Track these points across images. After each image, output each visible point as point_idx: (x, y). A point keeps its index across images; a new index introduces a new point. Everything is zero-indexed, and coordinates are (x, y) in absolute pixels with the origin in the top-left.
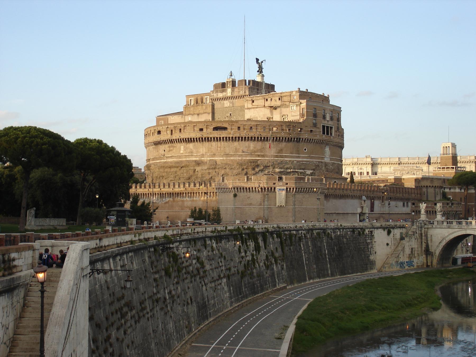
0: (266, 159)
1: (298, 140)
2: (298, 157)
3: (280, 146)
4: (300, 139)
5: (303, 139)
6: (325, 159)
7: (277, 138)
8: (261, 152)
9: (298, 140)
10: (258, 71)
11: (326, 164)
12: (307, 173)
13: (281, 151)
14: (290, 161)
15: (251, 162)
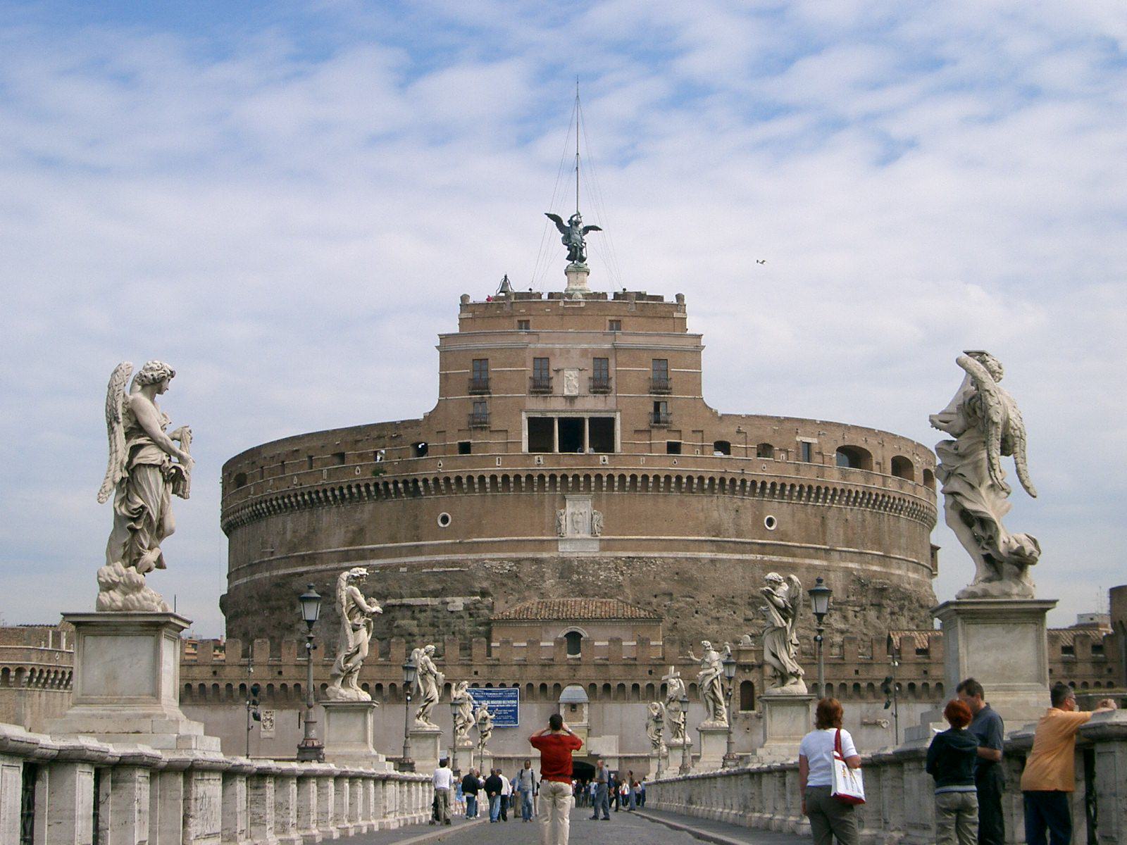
0: (320, 567)
1: (412, 488)
2: (417, 550)
3: (358, 515)
4: (415, 481)
5: (425, 481)
6: (561, 547)
7: (341, 489)
8: (309, 545)
9: (412, 488)
10: (569, 258)
11: (566, 568)
12: (450, 608)
13: (359, 535)
14: (383, 568)
15: (278, 585)
